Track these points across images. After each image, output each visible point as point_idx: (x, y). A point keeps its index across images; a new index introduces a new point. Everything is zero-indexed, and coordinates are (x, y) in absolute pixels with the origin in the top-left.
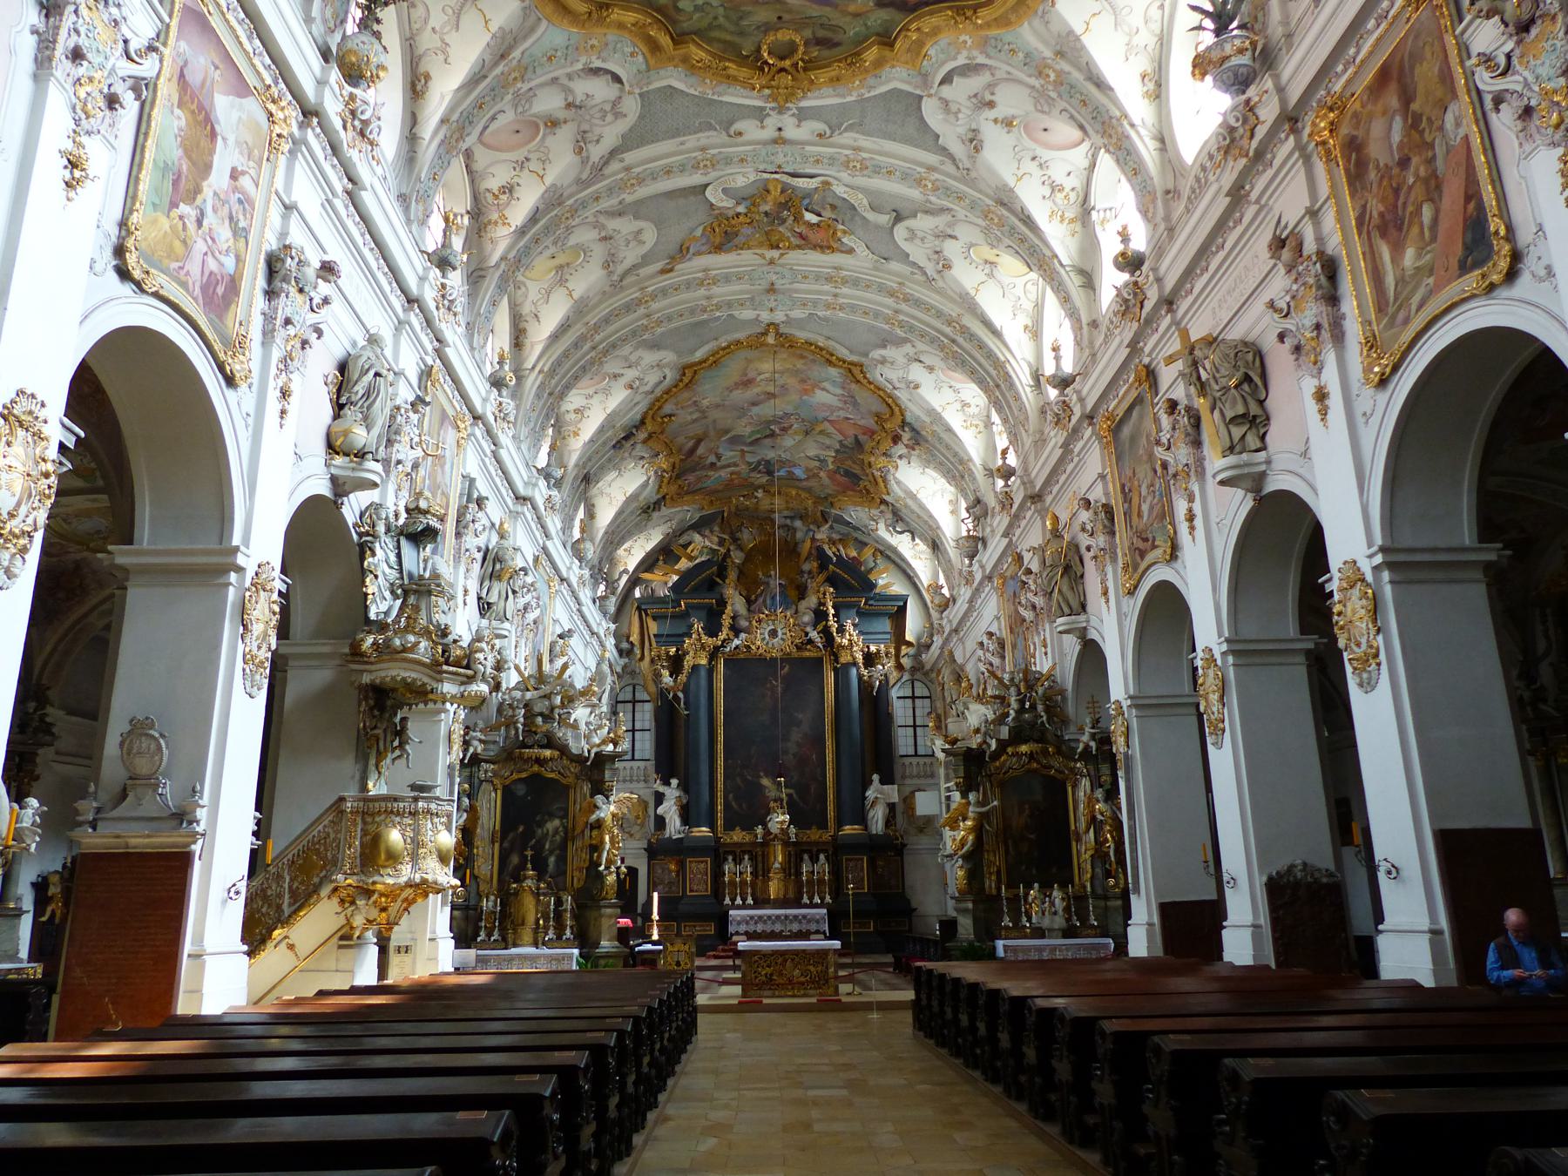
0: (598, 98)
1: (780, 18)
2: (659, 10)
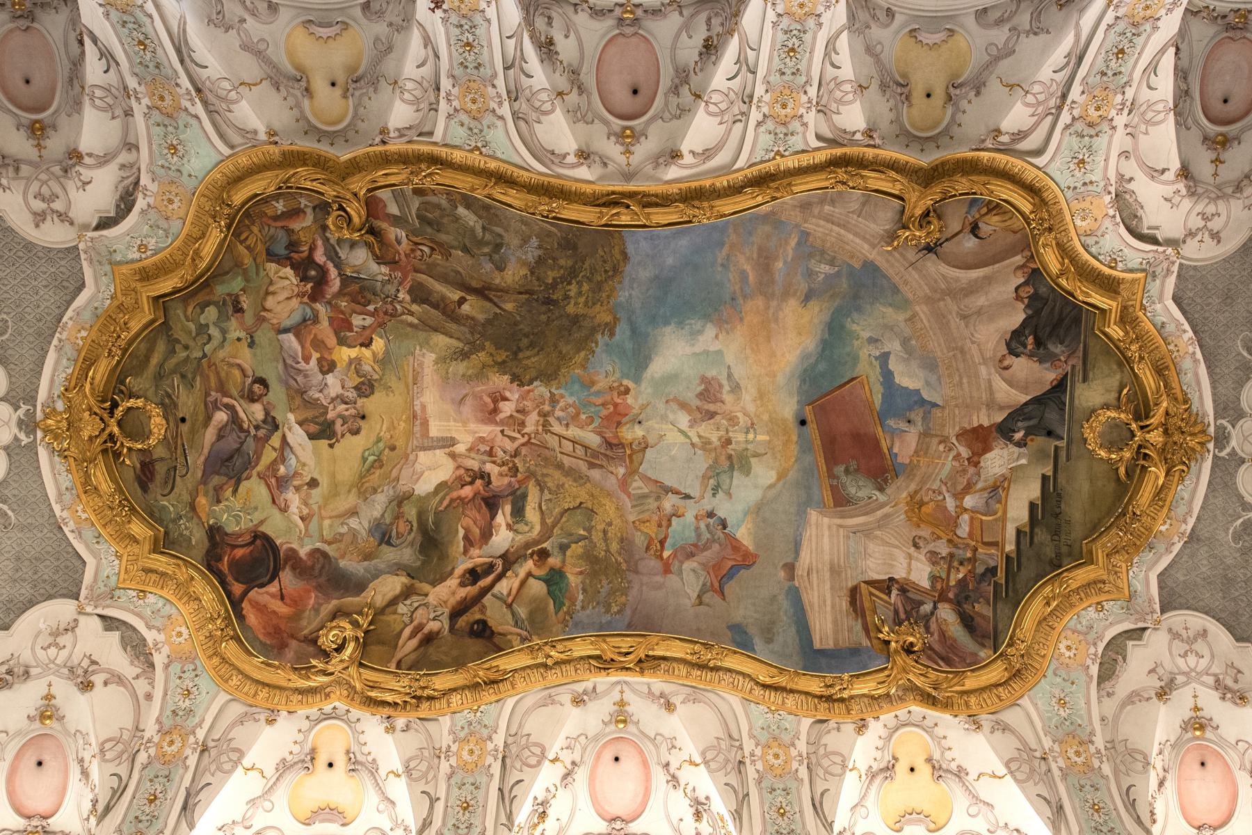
0: (73, 193)
1: (183, 420)
2: (206, 284)
